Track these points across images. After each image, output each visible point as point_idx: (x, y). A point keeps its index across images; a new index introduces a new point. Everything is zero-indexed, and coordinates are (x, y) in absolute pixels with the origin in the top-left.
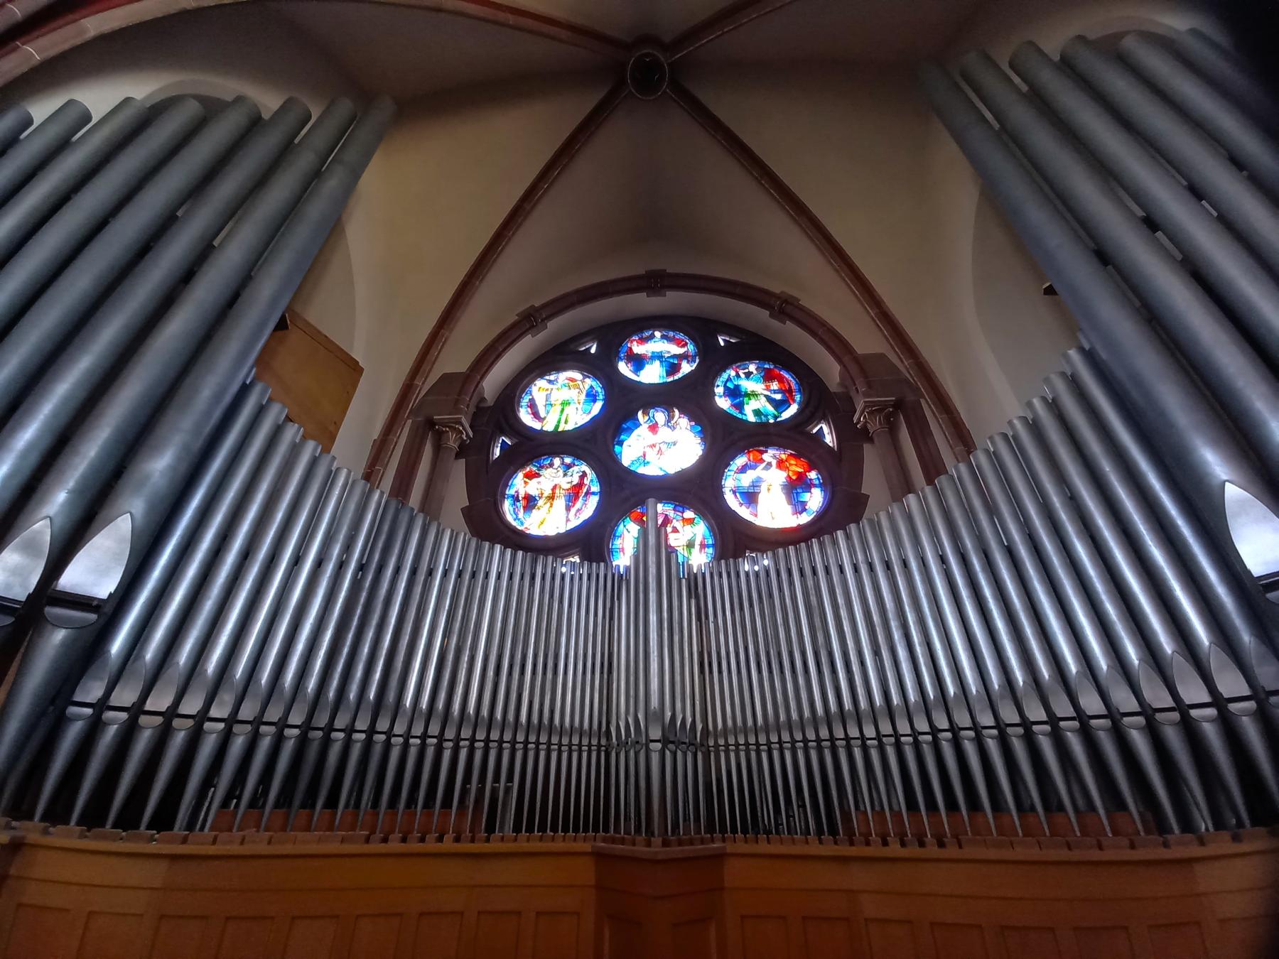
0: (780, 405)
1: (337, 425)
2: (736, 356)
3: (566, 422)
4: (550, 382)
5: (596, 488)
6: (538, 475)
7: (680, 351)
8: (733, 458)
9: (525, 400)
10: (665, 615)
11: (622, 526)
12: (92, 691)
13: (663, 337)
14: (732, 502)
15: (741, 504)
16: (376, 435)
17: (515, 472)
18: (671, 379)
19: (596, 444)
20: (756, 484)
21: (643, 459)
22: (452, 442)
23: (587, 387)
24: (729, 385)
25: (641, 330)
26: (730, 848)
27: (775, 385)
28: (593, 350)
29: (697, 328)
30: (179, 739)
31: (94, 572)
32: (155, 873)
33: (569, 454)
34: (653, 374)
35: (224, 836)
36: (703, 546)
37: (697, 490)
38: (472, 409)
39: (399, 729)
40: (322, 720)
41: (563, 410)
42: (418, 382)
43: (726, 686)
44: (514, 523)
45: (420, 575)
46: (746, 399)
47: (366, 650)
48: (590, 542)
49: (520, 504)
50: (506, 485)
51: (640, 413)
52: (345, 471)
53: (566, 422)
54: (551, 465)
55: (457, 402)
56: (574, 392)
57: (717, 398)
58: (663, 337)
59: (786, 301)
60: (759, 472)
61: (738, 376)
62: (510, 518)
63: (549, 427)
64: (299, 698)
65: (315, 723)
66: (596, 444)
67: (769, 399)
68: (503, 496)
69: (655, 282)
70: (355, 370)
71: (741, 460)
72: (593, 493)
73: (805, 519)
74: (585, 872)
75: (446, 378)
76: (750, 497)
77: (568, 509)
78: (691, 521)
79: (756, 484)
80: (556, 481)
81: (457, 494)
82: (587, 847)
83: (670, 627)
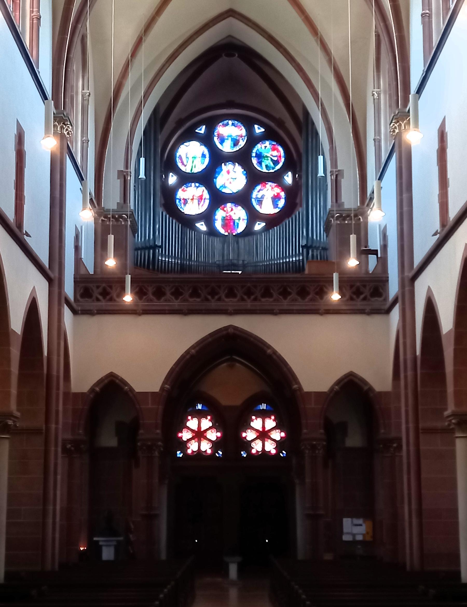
9: (178, 155)
19: (206, 178)
20: (263, 197)
24: (258, 152)
27: (275, 153)
29: (248, 123)
30: (167, 264)
34: (227, 148)
37: (243, 199)
43: (242, 258)
45: (191, 240)
48: (208, 217)
49: (182, 201)
51: (223, 164)
54: (191, 186)
57: (252, 158)
58: (233, 124)
63: (188, 171)
66: (206, 178)
67: (272, 160)
71: (259, 187)
73: (277, 210)
76: (260, 202)
77: (199, 204)
79: (263, 197)
83: (233, 249)
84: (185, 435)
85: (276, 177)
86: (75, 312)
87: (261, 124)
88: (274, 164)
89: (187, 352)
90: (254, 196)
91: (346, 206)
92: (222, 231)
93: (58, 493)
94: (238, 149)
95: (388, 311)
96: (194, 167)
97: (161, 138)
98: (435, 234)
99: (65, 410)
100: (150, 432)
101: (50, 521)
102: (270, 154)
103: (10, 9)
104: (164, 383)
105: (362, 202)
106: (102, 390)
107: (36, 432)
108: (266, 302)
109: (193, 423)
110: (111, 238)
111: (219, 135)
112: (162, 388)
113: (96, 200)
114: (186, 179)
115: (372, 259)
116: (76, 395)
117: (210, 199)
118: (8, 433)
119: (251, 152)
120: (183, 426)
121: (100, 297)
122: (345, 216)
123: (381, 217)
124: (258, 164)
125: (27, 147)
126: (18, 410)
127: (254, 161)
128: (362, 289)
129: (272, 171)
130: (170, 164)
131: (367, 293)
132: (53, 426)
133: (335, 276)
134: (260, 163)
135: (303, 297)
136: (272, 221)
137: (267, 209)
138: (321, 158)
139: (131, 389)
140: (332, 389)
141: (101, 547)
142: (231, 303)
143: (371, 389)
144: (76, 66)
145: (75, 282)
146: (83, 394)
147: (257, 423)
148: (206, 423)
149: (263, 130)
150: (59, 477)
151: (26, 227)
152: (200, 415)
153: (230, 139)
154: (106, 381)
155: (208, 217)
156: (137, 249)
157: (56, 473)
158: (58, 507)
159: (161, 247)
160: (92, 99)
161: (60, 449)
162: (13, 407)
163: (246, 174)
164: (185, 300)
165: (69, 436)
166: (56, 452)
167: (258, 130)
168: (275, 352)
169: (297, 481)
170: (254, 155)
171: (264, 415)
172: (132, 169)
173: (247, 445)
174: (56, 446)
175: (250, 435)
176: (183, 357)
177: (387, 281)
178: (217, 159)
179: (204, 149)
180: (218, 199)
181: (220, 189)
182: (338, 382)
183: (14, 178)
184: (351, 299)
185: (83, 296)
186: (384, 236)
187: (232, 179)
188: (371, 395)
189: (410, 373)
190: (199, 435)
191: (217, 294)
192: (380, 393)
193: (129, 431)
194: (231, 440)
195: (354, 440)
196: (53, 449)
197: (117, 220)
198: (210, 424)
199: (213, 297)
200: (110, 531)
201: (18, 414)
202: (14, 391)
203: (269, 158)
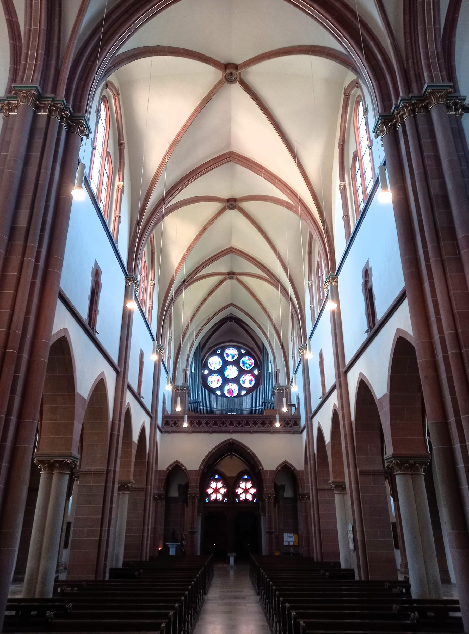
0: (250, 365)
2: (244, 355)
14: (241, 382)
19: (221, 372)
20: (245, 380)
21: (228, 375)
27: (250, 361)
28: (219, 352)
29: (239, 349)
34: (230, 359)
37: (236, 380)
43: (236, 407)
45: (214, 399)
48: (221, 388)
63: (213, 369)
66: (221, 372)
69: (231, 341)
73: (251, 386)
76: (244, 382)
79: (245, 380)
83: (232, 403)
84: (210, 491)
85: (250, 372)
86: (161, 432)
87: (244, 349)
89: (211, 451)
91: (281, 385)
92: (227, 395)
93: (150, 520)
95: (301, 432)
97: (202, 355)
98: (320, 398)
99: (155, 479)
100: (194, 490)
101: (146, 535)
102: (248, 362)
103: (141, 304)
104: (201, 466)
105: (288, 383)
106: (172, 469)
107: (142, 490)
108: (247, 428)
109: (213, 485)
110: (179, 399)
111: (226, 354)
112: (200, 468)
113: (173, 381)
114: (212, 372)
115: (293, 409)
116: (160, 471)
118: (128, 490)
120: (209, 486)
121: (173, 425)
122: (281, 389)
123: (296, 389)
125: (145, 360)
126: (134, 479)
127: (241, 365)
128: (289, 422)
130: (205, 366)
131: (292, 424)
132: (150, 487)
133: (277, 416)
134: (244, 366)
135: (263, 426)
136: (249, 391)
137: (247, 385)
138: (270, 364)
139: (186, 469)
140: (277, 469)
141: (169, 547)
142: (231, 428)
143: (295, 469)
144: (167, 326)
145: (162, 418)
146: (163, 471)
147: (243, 485)
148: (220, 485)
149: (245, 352)
150: (151, 512)
151: (142, 394)
152: (217, 480)
154: (174, 465)
156: (190, 403)
157: (149, 511)
158: (150, 528)
159: (200, 402)
160: (173, 339)
161: (152, 498)
162: (132, 478)
164: (210, 427)
165: (157, 492)
166: (150, 499)
167: (243, 351)
168: (251, 451)
169: (262, 514)
171: (246, 481)
172: (189, 368)
173: (238, 496)
174: (150, 497)
175: (239, 491)
176: (209, 453)
177: (300, 418)
178: (226, 363)
180: (226, 381)
182: (280, 466)
183: (138, 373)
184: (285, 426)
185: (165, 424)
186: (298, 398)
187: (231, 372)
188: (295, 472)
189: (312, 462)
190: (216, 491)
191: (225, 424)
192: (299, 471)
193: (184, 489)
194: (231, 494)
195: (288, 494)
196: (149, 498)
197: (182, 390)
198: (222, 485)
199: (223, 425)
200: (174, 540)
201: (134, 481)
202: (132, 470)
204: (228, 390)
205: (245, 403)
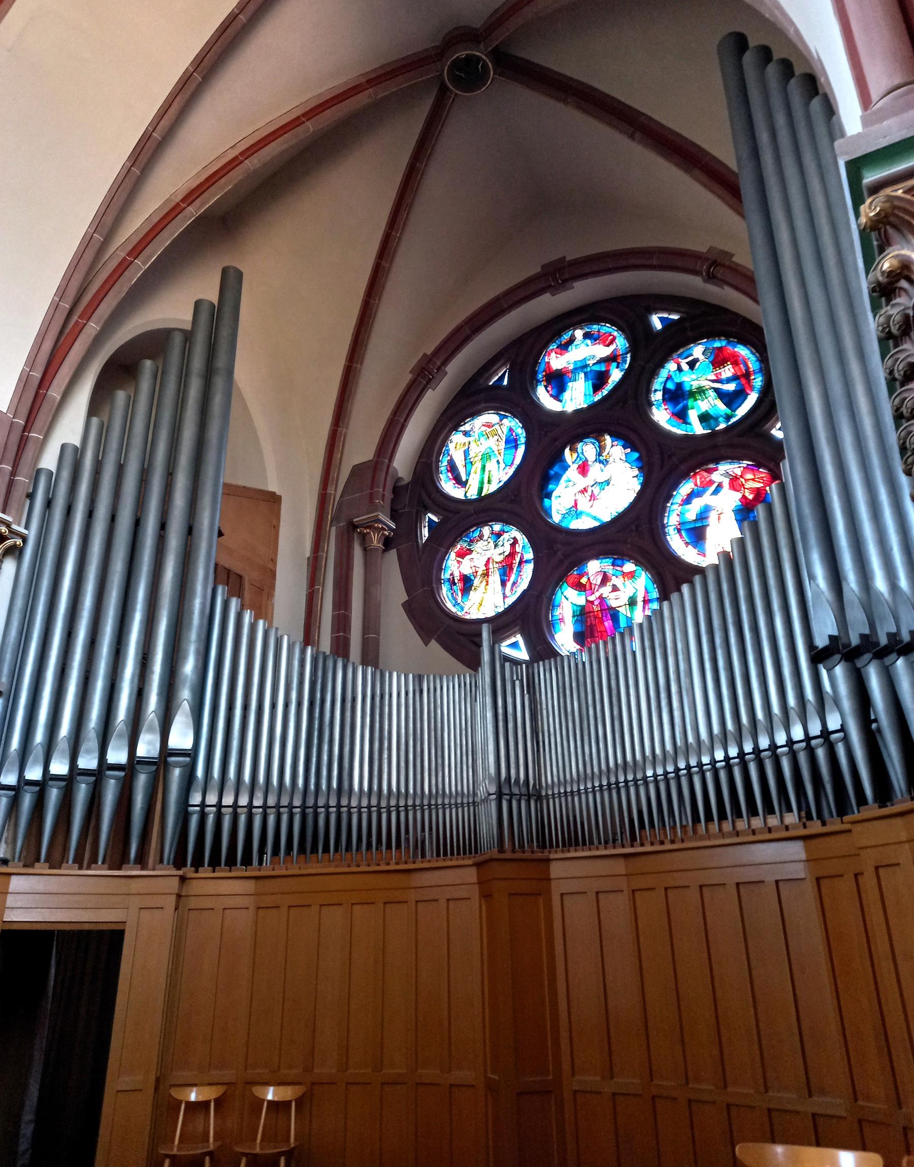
0: (731, 400)
1: (274, 561)
3: (489, 482)
4: (466, 434)
5: (529, 555)
6: (470, 552)
7: (603, 351)
8: (676, 486)
10: (500, 711)
11: (559, 594)
12: (196, 799)
13: (587, 336)
15: (687, 544)
16: (308, 553)
17: (447, 553)
18: (598, 397)
20: (703, 516)
22: (376, 541)
23: (505, 430)
24: (670, 386)
25: (559, 334)
26: (552, 856)
27: (727, 371)
28: (505, 382)
29: (625, 312)
30: (243, 819)
31: (181, 737)
32: (250, 886)
33: (497, 520)
35: (276, 867)
36: (646, 602)
38: (389, 495)
39: (354, 803)
40: (310, 802)
41: (484, 468)
42: (331, 490)
44: (454, 610)
45: (349, 703)
46: (690, 402)
47: (325, 757)
48: (530, 616)
49: (459, 585)
50: (440, 569)
51: (567, 451)
52: (285, 638)
53: (489, 482)
54: (481, 537)
55: (371, 497)
56: (492, 441)
58: (587, 336)
59: (715, 263)
60: (707, 499)
61: (680, 369)
62: (449, 605)
63: (472, 494)
64: (296, 791)
65: (307, 805)
67: (721, 394)
68: (439, 581)
69: (556, 275)
70: (274, 500)
71: (686, 488)
72: (527, 562)
74: (471, 875)
75: (357, 470)
76: (697, 534)
77: (503, 584)
78: (631, 575)
79: (703, 516)
80: (488, 555)
81: (394, 591)
82: (470, 862)
88: (728, 405)
90: (672, 520)
94: (605, 392)
96: (486, 480)
117: (537, 560)
119: (648, 391)
124: (675, 421)
127: (661, 416)
129: (722, 426)
134: (681, 416)
153: (582, 375)
155: (530, 616)
163: (638, 459)
170: (657, 397)
179: (513, 424)
181: (564, 525)
203: (712, 394)
204: (583, 615)
205: (637, 699)
